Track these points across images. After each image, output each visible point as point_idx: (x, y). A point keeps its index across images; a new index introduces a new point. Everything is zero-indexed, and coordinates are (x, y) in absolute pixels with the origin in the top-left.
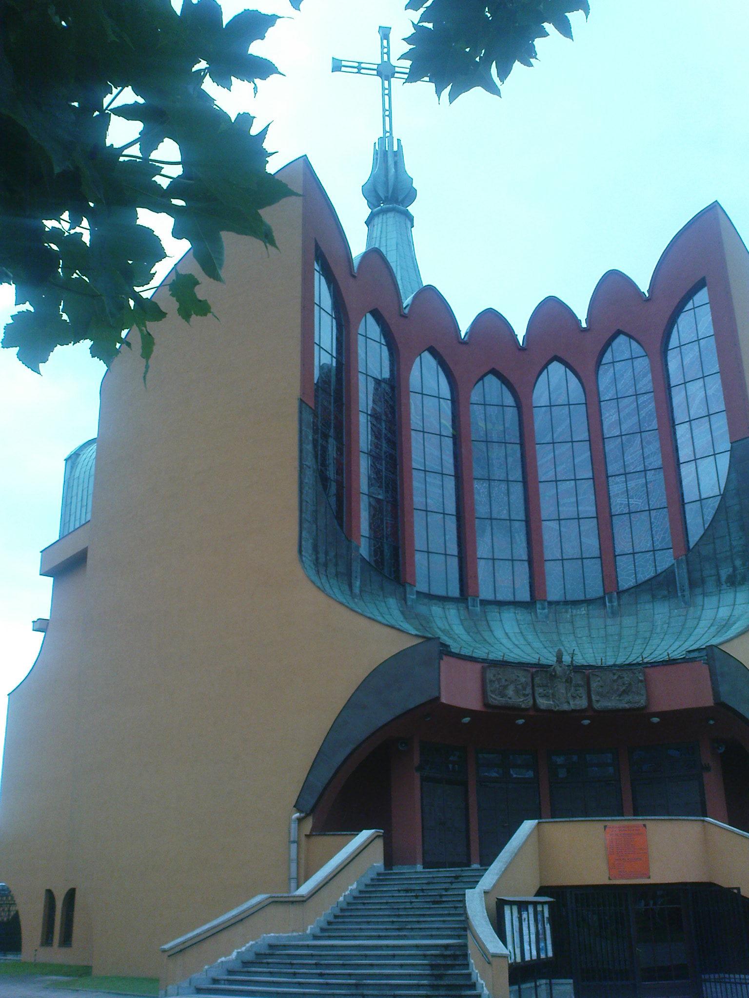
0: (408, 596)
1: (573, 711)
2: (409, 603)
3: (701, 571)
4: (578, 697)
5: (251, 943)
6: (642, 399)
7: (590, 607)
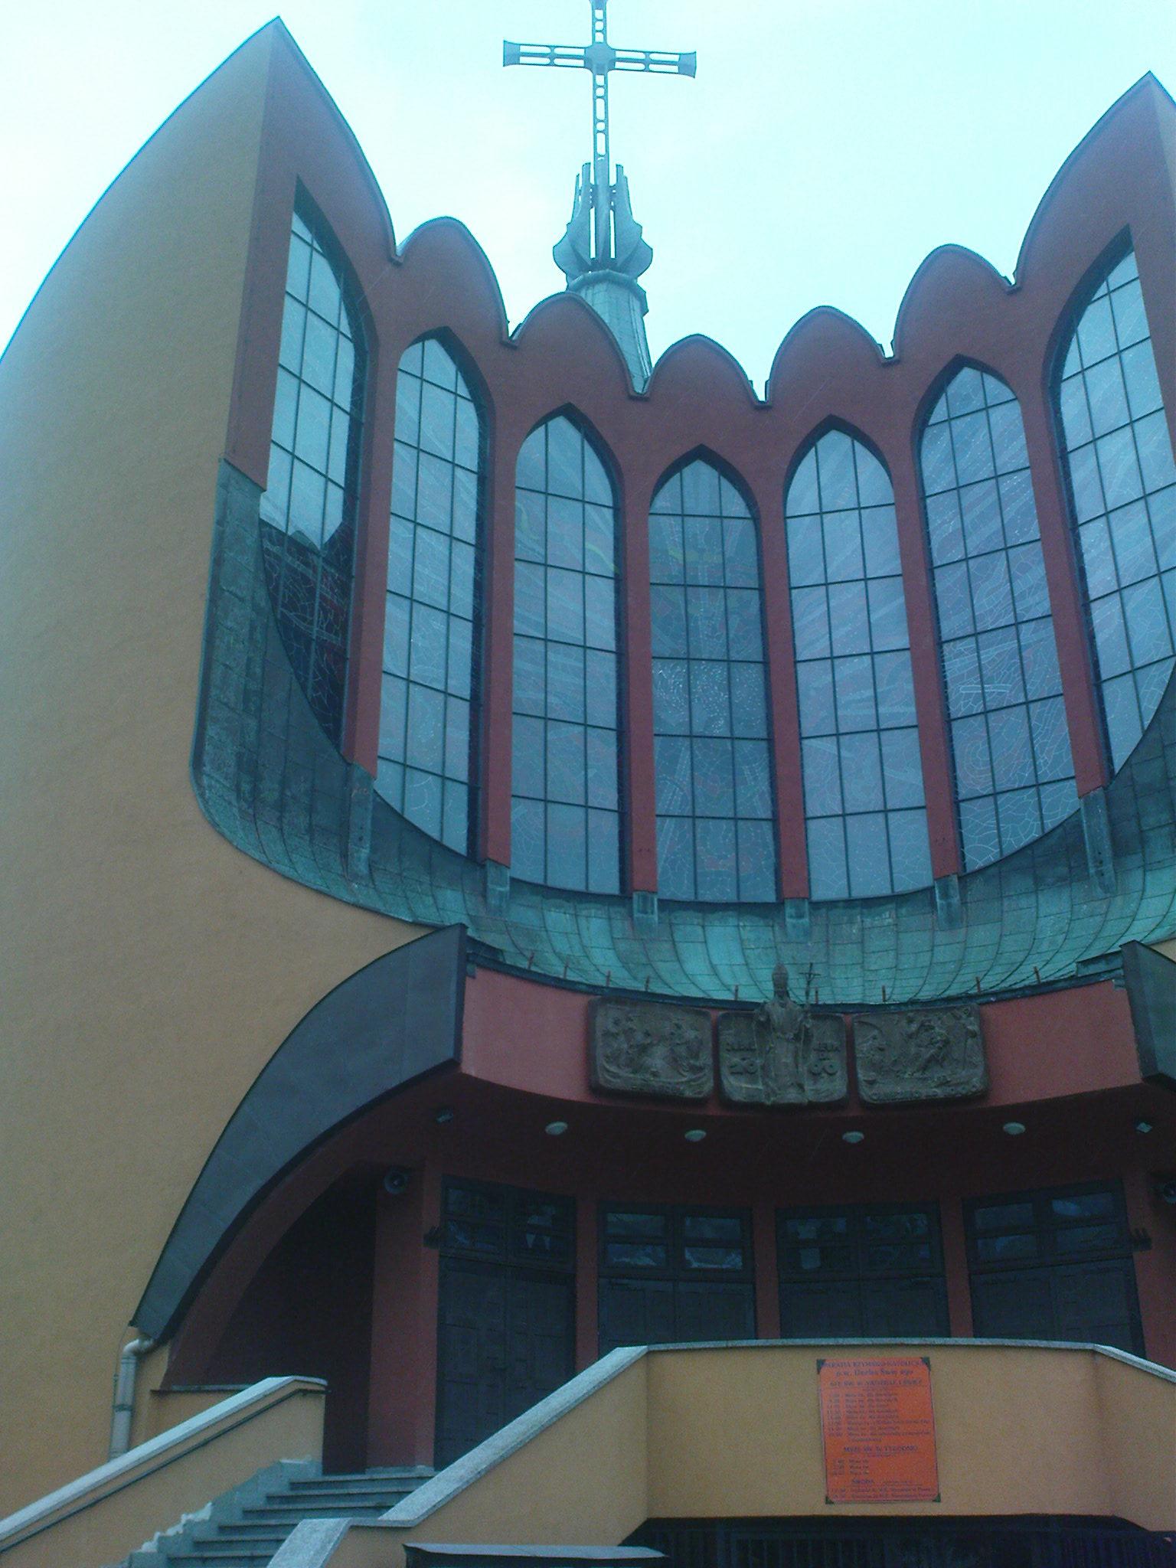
0: (490, 885)
1: (813, 1106)
2: (493, 902)
3: (1138, 817)
4: (824, 1075)
6: (1006, 485)
7: (904, 911)
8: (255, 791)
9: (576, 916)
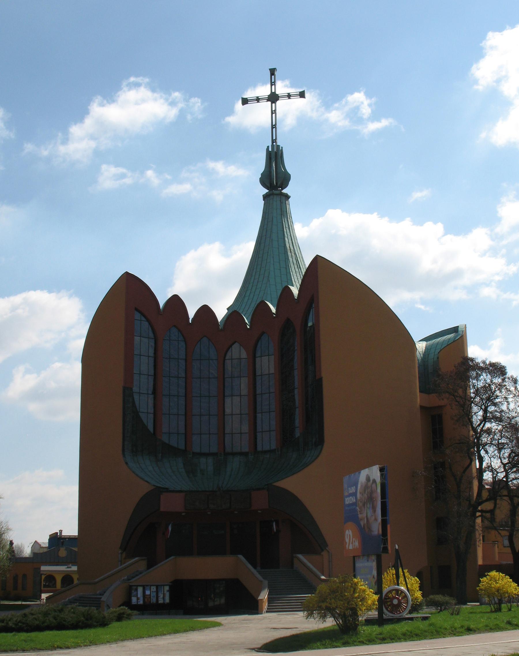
5: (73, 596)
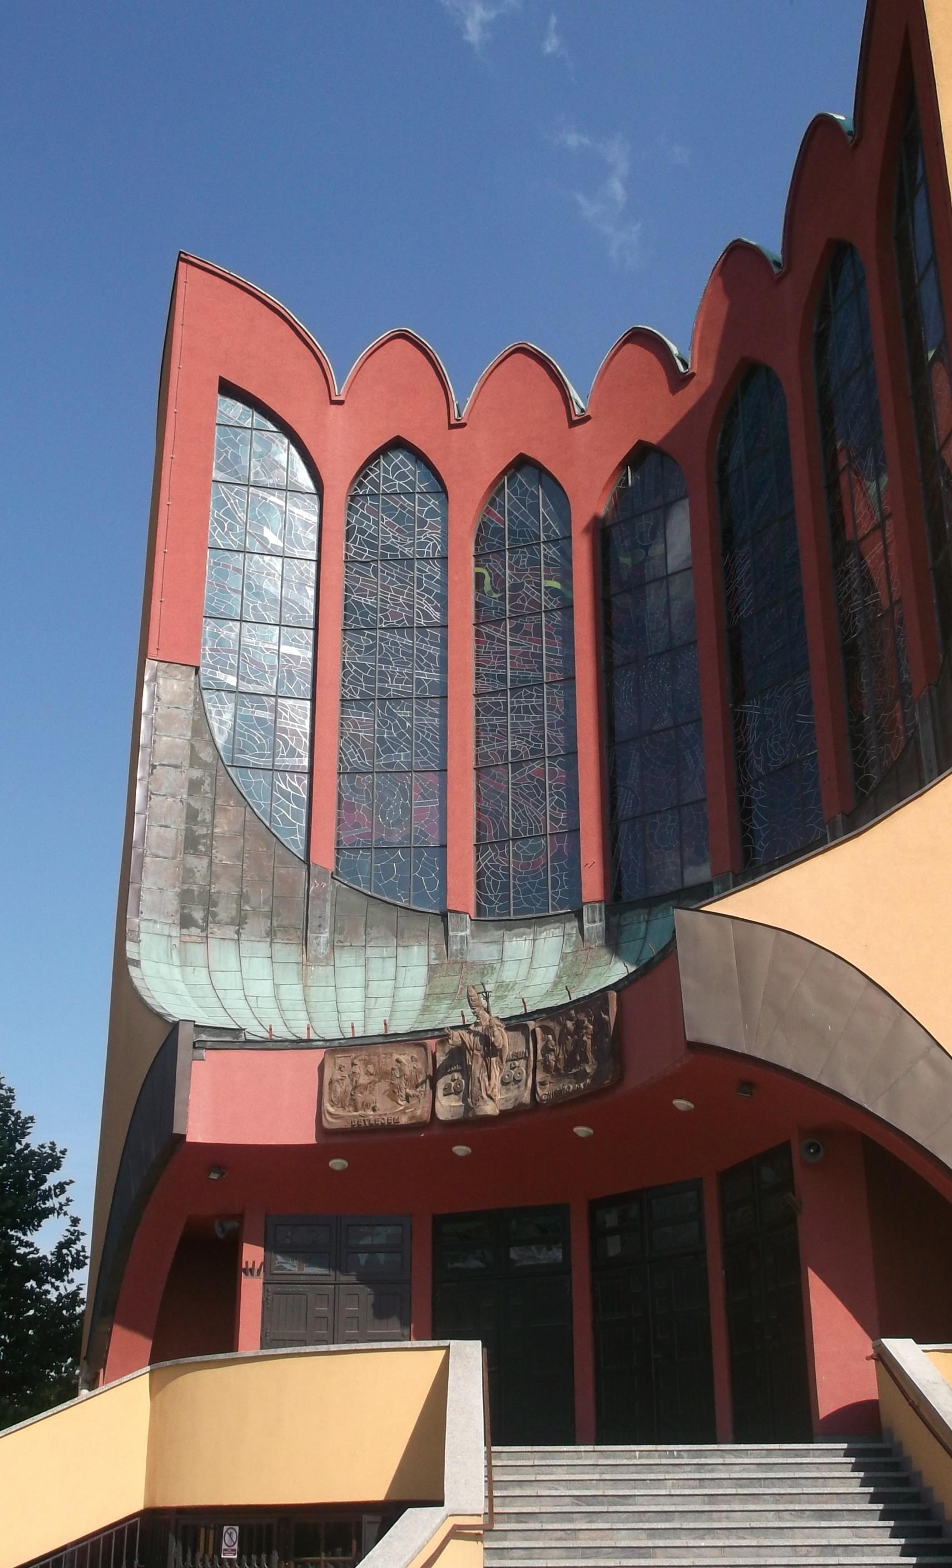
2: (454, 947)
8: (210, 916)
9: (534, 940)
